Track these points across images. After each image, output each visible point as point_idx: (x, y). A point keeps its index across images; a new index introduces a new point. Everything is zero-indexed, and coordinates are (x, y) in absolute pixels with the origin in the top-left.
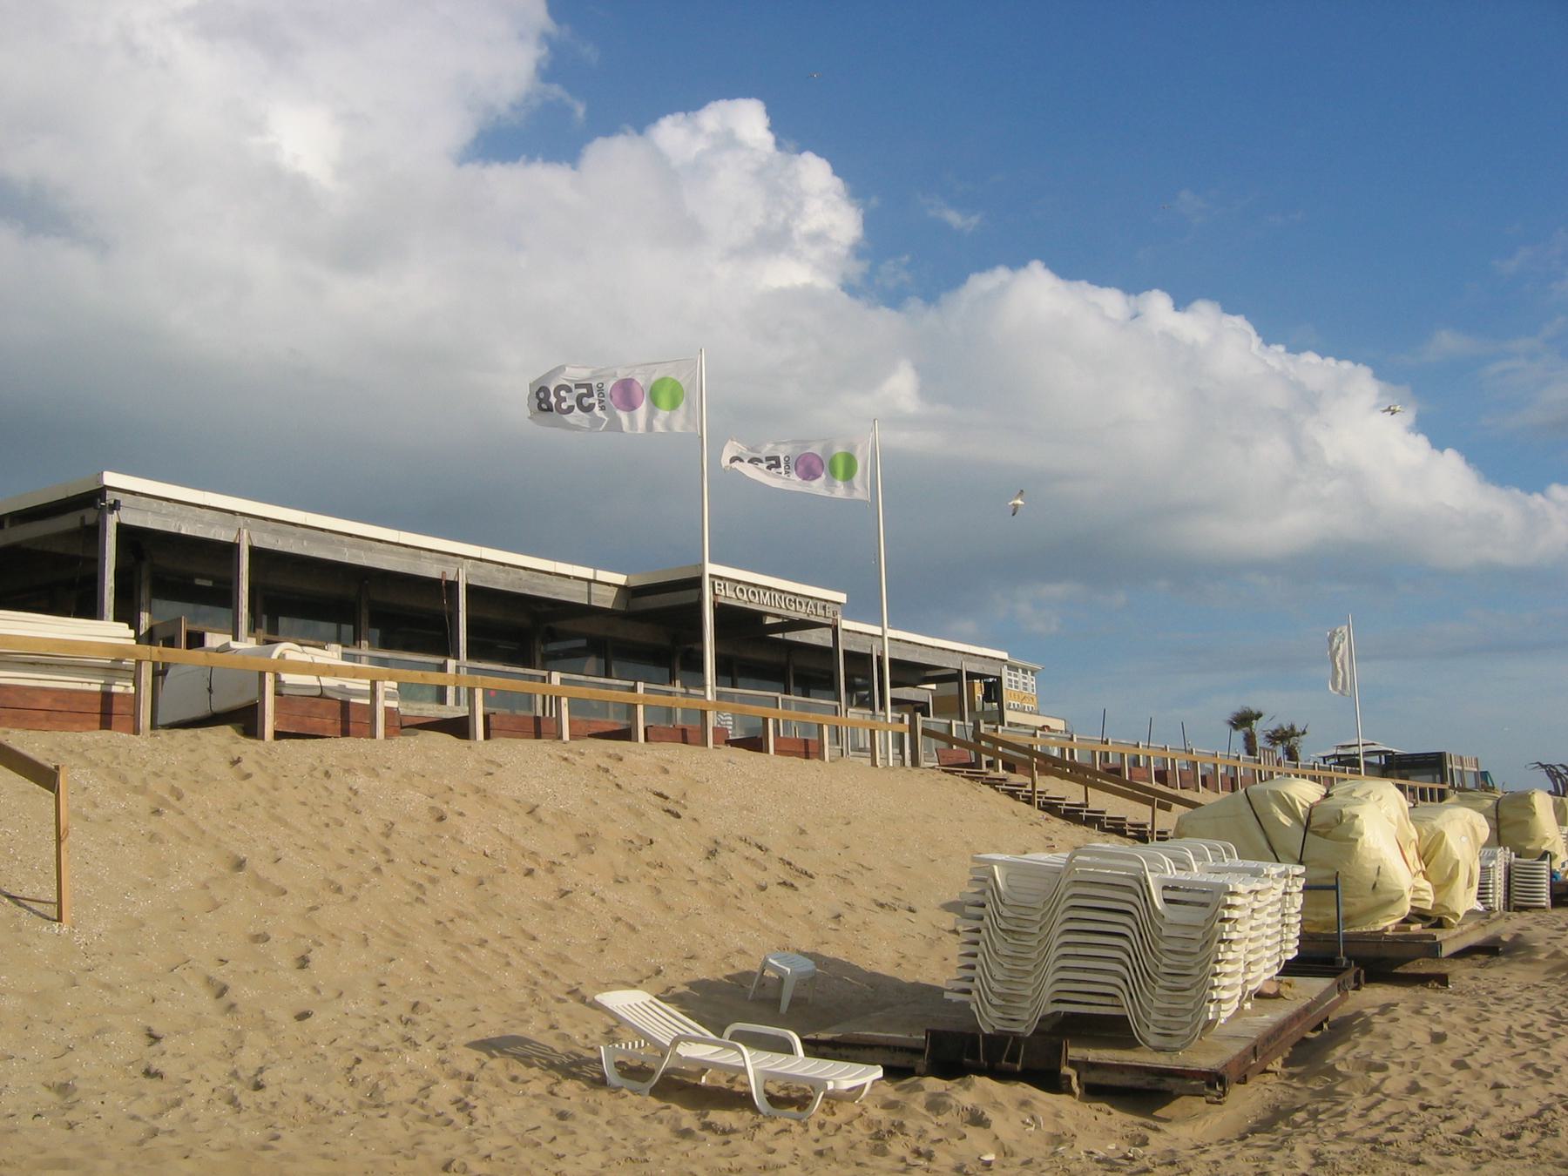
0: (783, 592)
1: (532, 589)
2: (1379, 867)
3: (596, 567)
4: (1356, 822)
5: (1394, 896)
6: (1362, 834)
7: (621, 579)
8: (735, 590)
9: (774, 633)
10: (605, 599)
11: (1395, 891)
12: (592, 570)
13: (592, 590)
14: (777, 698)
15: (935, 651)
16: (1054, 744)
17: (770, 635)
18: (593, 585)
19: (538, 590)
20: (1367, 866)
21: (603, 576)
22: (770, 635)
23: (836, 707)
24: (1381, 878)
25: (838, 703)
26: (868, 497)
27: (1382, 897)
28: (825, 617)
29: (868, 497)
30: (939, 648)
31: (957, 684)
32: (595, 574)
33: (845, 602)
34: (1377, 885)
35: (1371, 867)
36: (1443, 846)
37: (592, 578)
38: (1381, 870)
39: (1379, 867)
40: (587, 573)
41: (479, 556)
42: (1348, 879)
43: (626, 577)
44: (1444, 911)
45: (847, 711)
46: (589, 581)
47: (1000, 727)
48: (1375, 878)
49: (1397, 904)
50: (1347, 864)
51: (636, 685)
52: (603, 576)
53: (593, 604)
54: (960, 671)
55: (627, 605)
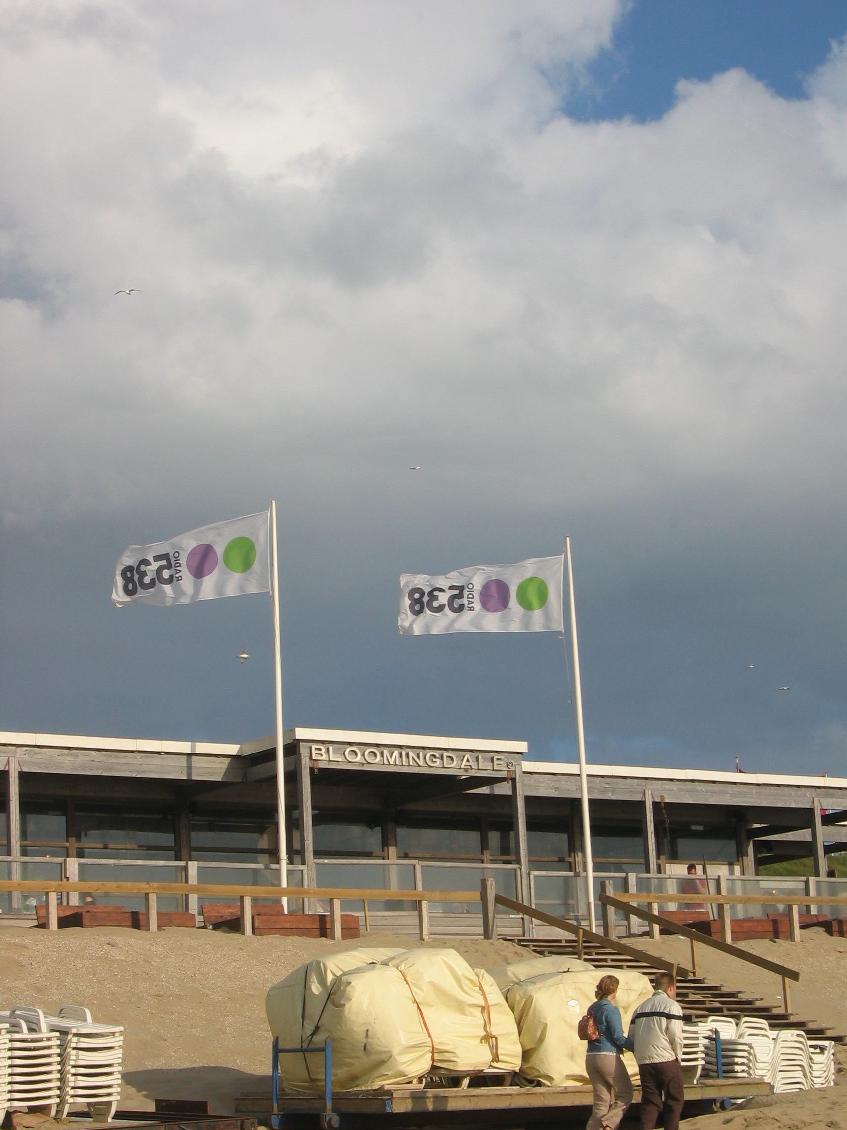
0: (400, 746)
1: (106, 770)
2: (368, 1030)
3: (193, 739)
4: (348, 989)
5: (384, 1057)
6: (350, 1000)
7: (232, 749)
8: (344, 754)
9: (468, 790)
10: (214, 772)
11: (384, 1052)
12: (189, 743)
13: (194, 764)
14: (414, 866)
15: (763, 790)
16: (780, 901)
17: (468, 792)
18: (194, 758)
19: (118, 771)
20: (355, 1029)
21: (203, 747)
22: (468, 792)
23: (515, 870)
24: (370, 1040)
25: (518, 866)
26: (561, 628)
27: (375, 1058)
28: (493, 770)
29: (561, 628)
30: (764, 785)
31: (809, 830)
32: (193, 747)
33: (527, 751)
34: (368, 1047)
35: (359, 1030)
36: (532, 1009)
37: (189, 751)
38: (369, 1033)
39: (368, 1030)
40: (184, 747)
41: (34, 744)
42: (343, 1041)
43: (239, 746)
44: (536, 1074)
45: (529, 874)
46: (189, 755)
47: (812, 880)
48: (364, 1041)
49: (388, 1063)
50: (340, 1027)
51: (187, 864)
52: (203, 747)
53: (194, 778)
54: (811, 811)
55: (245, 775)
